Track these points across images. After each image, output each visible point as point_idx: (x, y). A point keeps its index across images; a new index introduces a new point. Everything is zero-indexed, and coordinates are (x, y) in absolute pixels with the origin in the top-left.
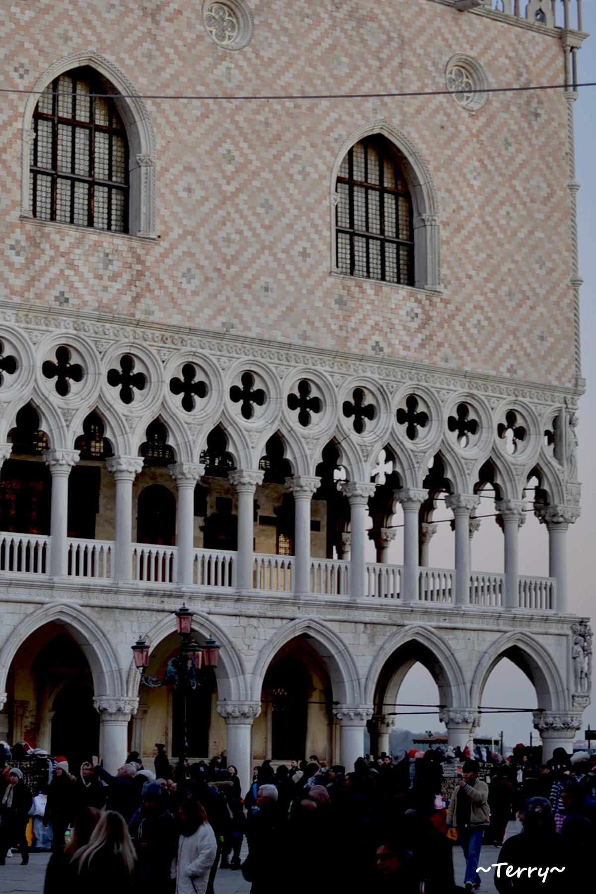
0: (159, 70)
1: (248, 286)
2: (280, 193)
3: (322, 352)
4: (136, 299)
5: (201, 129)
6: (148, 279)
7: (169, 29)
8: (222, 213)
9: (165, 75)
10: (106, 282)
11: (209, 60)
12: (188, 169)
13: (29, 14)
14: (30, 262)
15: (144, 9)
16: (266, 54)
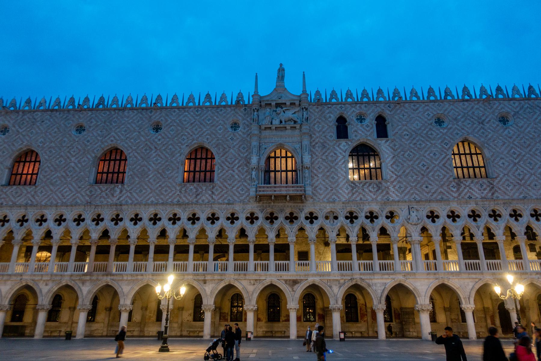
0: (487, 136)
1: (529, 185)
2: (534, 159)
4: (493, 194)
5: (504, 148)
6: (495, 188)
7: (488, 125)
8: (515, 168)
9: (490, 136)
10: (482, 191)
11: (502, 130)
12: (502, 158)
13: (445, 131)
14: (458, 190)
15: (479, 122)
16: (520, 125)
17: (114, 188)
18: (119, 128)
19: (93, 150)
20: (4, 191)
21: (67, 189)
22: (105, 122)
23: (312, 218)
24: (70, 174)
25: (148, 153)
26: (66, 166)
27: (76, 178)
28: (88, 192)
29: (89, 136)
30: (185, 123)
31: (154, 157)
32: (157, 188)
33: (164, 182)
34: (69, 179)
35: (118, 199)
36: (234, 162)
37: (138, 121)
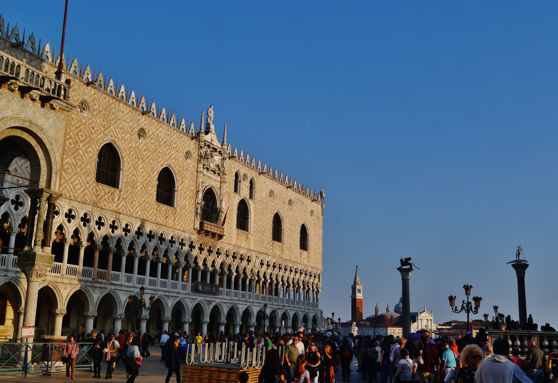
3: (298, 263)
17: (114, 191)
18: (116, 122)
19: (98, 141)
20: (20, 164)
21: (77, 182)
22: (105, 109)
23: (218, 253)
24: (79, 164)
25: (137, 163)
26: (76, 151)
27: (84, 171)
28: (94, 190)
29: (93, 121)
30: (161, 139)
31: (141, 168)
32: (143, 203)
33: (147, 198)
34: (79, 170)
35: (117, 206)
36: (187, 192)
37: (130, 122)
